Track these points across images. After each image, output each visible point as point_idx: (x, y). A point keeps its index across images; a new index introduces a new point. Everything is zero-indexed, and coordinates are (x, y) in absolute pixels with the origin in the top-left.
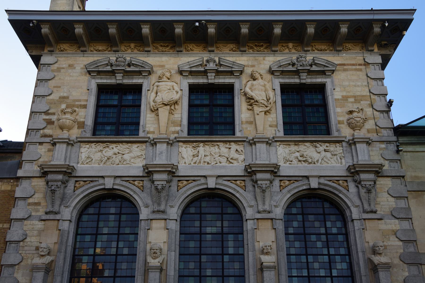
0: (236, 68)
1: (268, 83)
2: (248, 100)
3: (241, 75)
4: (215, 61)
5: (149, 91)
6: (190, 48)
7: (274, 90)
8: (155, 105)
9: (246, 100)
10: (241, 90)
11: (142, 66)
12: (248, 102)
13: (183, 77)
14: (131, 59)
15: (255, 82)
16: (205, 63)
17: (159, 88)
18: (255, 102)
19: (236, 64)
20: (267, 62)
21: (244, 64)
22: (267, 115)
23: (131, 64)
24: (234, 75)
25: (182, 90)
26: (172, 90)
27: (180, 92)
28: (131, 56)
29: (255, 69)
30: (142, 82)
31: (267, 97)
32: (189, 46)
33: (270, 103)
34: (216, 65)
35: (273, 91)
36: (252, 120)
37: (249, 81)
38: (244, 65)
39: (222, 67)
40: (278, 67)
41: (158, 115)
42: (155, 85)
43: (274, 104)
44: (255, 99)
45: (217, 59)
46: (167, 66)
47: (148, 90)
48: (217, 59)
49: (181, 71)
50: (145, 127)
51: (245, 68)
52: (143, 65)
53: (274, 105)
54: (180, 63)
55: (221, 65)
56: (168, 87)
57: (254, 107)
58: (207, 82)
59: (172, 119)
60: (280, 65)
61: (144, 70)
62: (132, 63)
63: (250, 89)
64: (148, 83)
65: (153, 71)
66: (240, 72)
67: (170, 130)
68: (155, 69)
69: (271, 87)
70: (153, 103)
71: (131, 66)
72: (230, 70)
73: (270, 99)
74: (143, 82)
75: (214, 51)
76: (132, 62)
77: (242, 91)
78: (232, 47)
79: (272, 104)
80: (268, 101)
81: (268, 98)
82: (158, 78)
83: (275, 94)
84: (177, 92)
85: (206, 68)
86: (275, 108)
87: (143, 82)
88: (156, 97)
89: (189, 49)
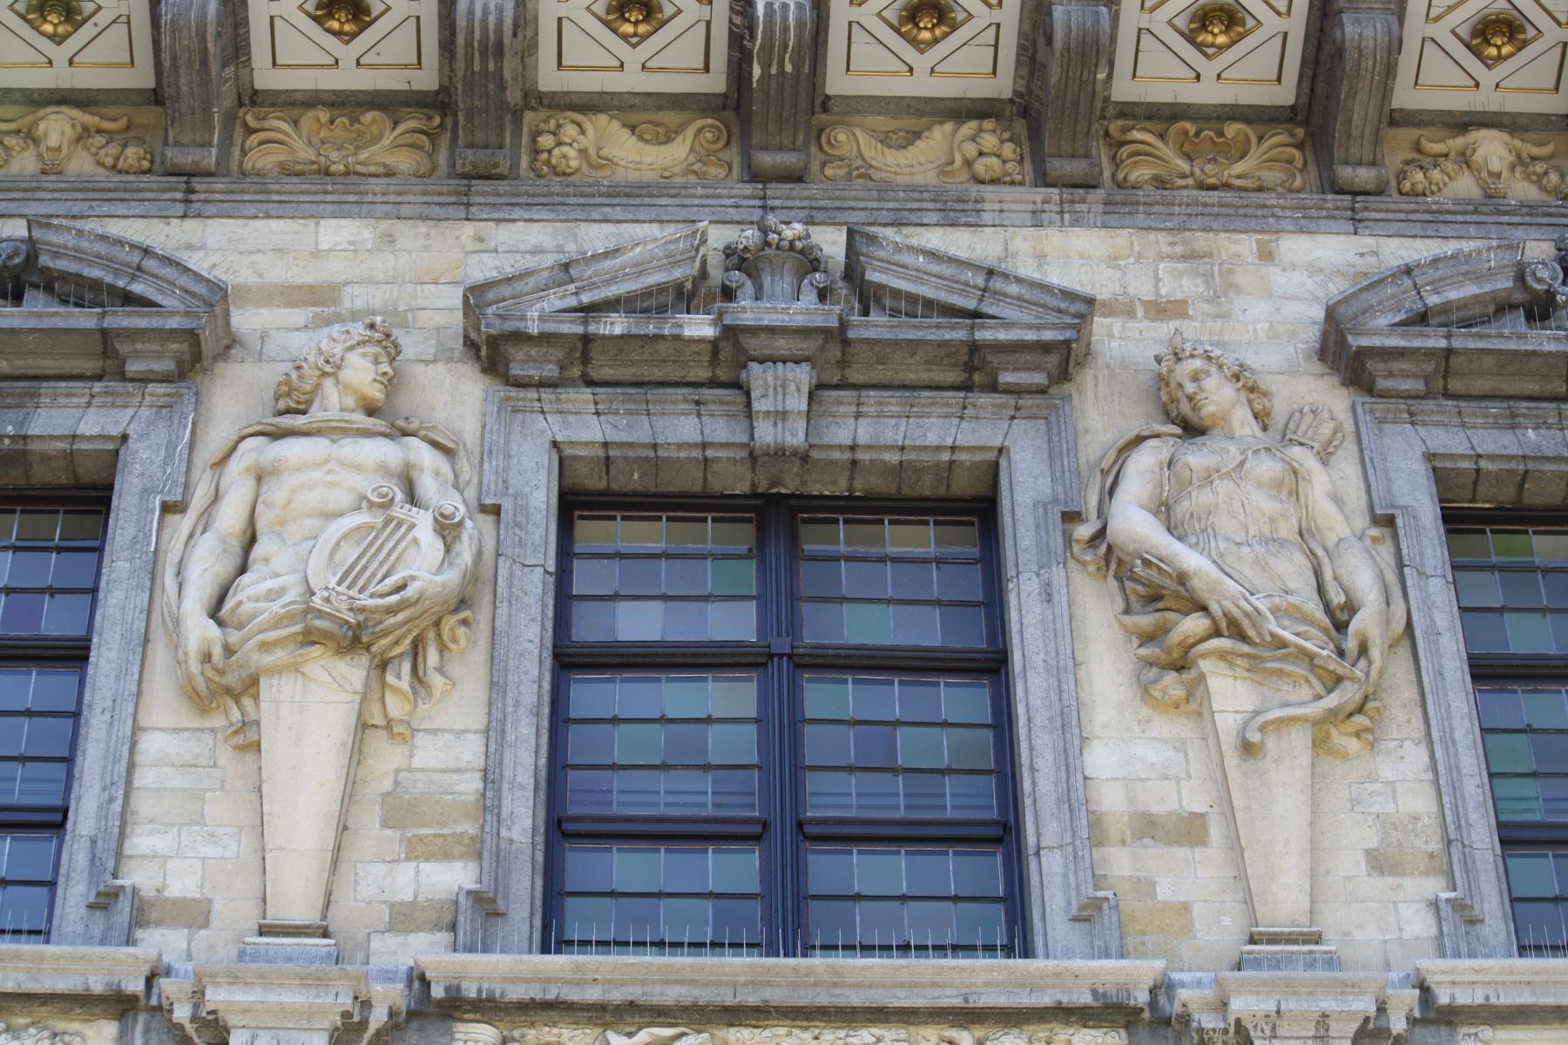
0: (1009, 325)
1: (1325, 457)
2: (1145, 621)
3: (1066, 387)
4: (809, 262)
5: (172, 519)
6: (583, 152)
7: (1389, 522)
8: (229, 651)
9: (1127, 611)
10: (1071, 517)
11: (128, 299)
12: (1148, 638)
13: (513, 392)
14: (37, 234)
15: (1197, 458)
16: (716, 275)
17: (277, 492)
18: (1217, 633)
19: (1013, 289)
20: (1298, 276)
21: (1087, 290)
22: (1343, 756)
23: (35, 279)
24: (993, 387)
25: (496, 511)
26: (401, 510)
27: (477, 531)
28: (32, 209)
29: (1193, 330)
30: (115, 431)
31: (1321, 590)
32: (570, 131)
33: (1363, 650)
34: (823, 294)
35: (1375, 532)
36: (1200, 808)
37: (1139, 440)
38: (1090, 301)
39: (874, 317)
40: (1402, 324)
41: (257, 747)
42: (236, 466)
43: (1404, 652)
44: (1215, 608)
45: (831, 243)
46: (356, 298)
47: (167, 508)
48: (831, 243)
49: (494, 342)
50: (119, 855)
51: (1099, 323)
52: (138, 288)
53: (1401, 671)
54: (482, 269)
55: (868, 297)
56: (368, 485)
57: (1212, 682)
58: (742, 438)
59: (386, 785)
60: (1419, 307)
61: (142, 323)
62: (46, 270)
63: (1163, 510)
64: (171, 446)
65: (230, 344)
66: (1053, 360)
67: (367, 890)
68: (245, 320)
69: (1355, 494)
70: (213, 629)
71: (29, 295)
72: (960, 335)
73: (1351, 608)
74: (125, 438)
75: (800, 180)
76: (45, 260)
77: (1084, 531)
78: (970, 150)
79: (1375, 653)
80: (1341, 627)
81: (1338, 598)
82: (269, 396)
83: (1401, 566)
84: (447, 529)
85: (728, 320)
86: (1408, 692)
87: (125, 438)
88: (243, 569)
89: (571, 152)
